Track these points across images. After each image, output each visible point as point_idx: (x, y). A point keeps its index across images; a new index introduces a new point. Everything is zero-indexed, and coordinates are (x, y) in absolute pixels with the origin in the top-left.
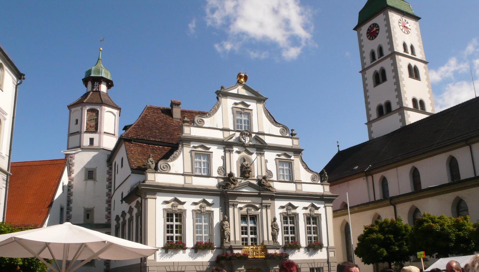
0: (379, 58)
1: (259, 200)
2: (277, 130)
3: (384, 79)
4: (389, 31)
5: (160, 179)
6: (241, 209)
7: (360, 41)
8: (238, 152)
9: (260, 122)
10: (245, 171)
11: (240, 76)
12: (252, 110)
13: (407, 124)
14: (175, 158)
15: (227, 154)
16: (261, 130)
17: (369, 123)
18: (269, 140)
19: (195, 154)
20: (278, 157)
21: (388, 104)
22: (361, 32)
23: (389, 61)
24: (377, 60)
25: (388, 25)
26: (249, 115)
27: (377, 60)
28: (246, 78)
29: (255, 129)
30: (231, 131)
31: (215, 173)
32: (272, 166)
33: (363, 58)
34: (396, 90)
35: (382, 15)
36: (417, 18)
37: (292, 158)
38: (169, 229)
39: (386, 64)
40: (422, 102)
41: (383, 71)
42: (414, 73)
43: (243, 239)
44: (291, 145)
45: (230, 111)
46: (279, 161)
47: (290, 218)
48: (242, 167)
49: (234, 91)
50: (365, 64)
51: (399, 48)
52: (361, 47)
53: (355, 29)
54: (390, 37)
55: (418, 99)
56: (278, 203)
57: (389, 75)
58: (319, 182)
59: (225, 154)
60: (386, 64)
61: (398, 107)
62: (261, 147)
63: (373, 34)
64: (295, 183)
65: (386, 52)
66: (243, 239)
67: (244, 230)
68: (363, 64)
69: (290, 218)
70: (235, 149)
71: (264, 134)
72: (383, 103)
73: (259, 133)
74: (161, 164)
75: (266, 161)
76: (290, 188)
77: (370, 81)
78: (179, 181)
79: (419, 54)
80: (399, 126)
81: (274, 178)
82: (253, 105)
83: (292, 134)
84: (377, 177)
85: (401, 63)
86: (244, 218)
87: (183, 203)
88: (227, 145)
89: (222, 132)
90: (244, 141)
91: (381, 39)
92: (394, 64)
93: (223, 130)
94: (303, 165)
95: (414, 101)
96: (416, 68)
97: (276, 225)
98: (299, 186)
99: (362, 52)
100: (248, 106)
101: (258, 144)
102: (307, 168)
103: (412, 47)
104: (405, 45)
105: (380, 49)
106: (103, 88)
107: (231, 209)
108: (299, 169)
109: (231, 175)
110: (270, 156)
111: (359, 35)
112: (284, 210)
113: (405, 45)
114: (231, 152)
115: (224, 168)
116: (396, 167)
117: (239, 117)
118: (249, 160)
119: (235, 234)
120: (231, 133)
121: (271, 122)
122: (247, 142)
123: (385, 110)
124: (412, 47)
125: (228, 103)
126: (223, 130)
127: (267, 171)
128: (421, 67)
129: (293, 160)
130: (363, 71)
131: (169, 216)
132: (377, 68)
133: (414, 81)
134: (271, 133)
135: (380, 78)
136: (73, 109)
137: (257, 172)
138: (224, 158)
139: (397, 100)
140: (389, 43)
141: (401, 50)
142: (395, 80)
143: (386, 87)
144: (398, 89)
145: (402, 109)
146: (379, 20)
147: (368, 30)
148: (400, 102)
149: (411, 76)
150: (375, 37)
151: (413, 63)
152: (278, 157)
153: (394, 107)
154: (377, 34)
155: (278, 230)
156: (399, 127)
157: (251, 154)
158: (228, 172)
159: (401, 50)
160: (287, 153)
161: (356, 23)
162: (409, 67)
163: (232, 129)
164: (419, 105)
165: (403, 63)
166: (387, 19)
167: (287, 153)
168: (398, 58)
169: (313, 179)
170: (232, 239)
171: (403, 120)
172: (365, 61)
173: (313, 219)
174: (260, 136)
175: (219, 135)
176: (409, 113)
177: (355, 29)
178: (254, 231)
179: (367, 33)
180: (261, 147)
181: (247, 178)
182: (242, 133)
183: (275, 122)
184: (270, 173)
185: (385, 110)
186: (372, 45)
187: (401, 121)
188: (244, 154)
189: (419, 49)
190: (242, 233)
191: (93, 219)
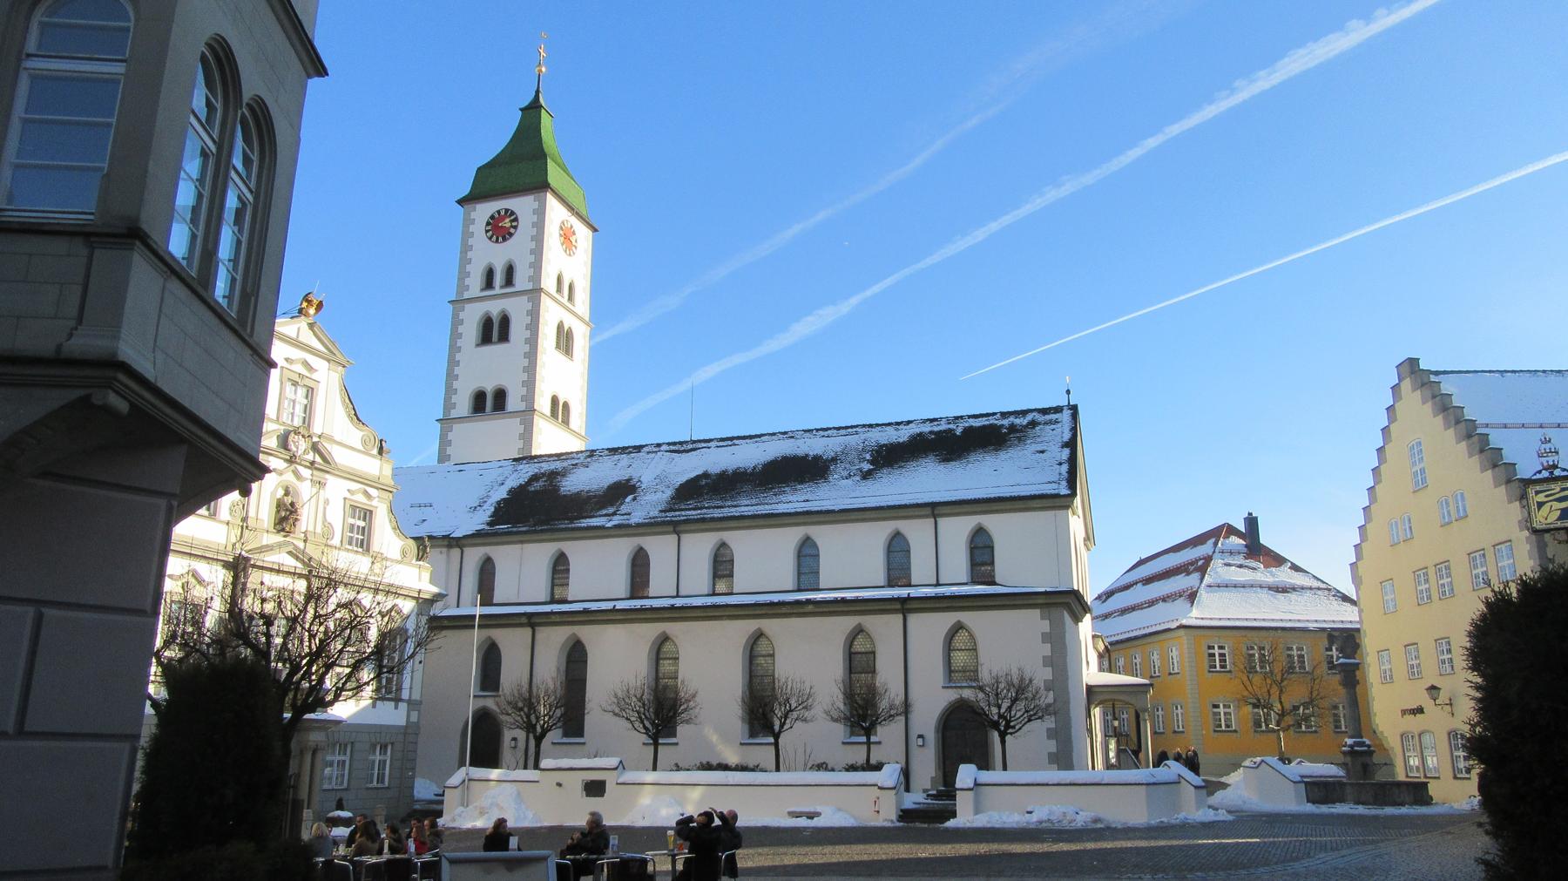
2: (355, 435)
3: (504, 337)
4: (539, 239)
7: (466, 234)
11: (306, 299)
17: (446, 422)
20: (348, 495)
21: (500, 396)
22: (473, 215)
24: (497, 290)
25: (540, 225)
26: (310, 392)
27: (497, 290)
28: (320, 306)
29: (317, 429)
33: (463, 274)
34: (525, 370)
35: (531, 198)
36: (595, 230)
37: (375, 503)
41: (505, 321)
44: (376, 473)
48: (280, 505)
50: (467, 288)
51: (548, 283)
53: (460, 202)
54: (538, 253)
57: (517, 330)
60: (516, 308)
61: (522, 406)
63: (500, 229)
65: (521, 281)
68: (462, 287)
71: (332, 440)
72: (489, 388)
75: (327, 502)
77: (471, 330)
83: (381, 451)
92: (534, 314)
95: (555, 401)
99: (465, 261)
103: (571, 287)
110: (337, 489)
111: (468, 221)
113: (559, 280)
116: (522, 542)
118: (297, 493)
123: (490, 403)
124: (571, 287)
130: (458, 303)
132: (494, 308)
133: (560, 357)
135: (494, 331)
139: (524, 391)
140: (531, 265)
142: (527, 348)
144: (531, 369)
145: (529, 412)
146: (522, 205)
147: (492, 217)
148: (529, 397)
149: (558, 346)
150: (504, 239)
151: (570, 322)
152: (348, 495)
153: (513, 403)
154: (511, 235)
160: (370, 490)
161: (465, 190)
162: (560, 327)
164: (560, 411)
165: (551, 314)
166: (541, 212)
167: (370, 490)
168: (546, 302)
169: (404, 554)
171: (527, 436)
172: (467, 282)
177: (460, 202)
179: (488, 224)
184: (328, 527)
185: (490, 403)
188: (289, 477)
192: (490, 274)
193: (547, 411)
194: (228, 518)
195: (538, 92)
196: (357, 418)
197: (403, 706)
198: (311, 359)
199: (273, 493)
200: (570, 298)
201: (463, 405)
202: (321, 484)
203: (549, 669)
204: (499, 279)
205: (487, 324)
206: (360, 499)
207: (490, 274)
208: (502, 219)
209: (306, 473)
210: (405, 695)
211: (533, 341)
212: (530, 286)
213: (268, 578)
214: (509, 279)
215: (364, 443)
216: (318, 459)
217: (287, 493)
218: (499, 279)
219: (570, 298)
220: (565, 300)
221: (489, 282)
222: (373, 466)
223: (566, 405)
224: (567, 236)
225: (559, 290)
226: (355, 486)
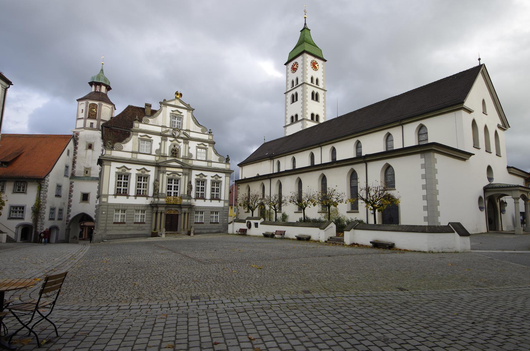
1: (181, 170)
2: (199, 129)
3: (297, 100)
5: (115, 154)
6: (168, 174)
7: (287, 73)
9: (188, 123)
10: (175, 152)
14: (127, 142)
15: (163, 142)
16: (188, 129)
18: (192, 135)
19: (142, 139)
21: (297, 116)
23: (300, 88)
24: (295, 86)
27: (295, 86)
29: (184, 128)
31: (154, 153)
37: (207, 147)
38: (119, 184)
39: (299, 90)
40: (317, 116)
41: (297, 94)
42: (315, 97)
43: (168, 193)
47: (201, 182)
49: (172, 103)
52: (287, 77)
55: (315, 114)
56: (195, 173)
63: (294, 69)
65: (300, 82)
66: (168, 193)
67: (169, 188)
68: (287, 88)
69: (201, 182)
70: (169, 139)
71: (189, 131)
73: (187, 130)
74: (117, 145)
75: (189, 148)
76: (204, 164)
77: (289, 100)
78: (128, 156)
79: (321, 85)
81: (194, 157)
82: (184, 112)
84: (276, 161)
86: (170, 180)
87: (130, 169)
88: (163, 136)
91: (298, 73)
93: (162, 126)
95: (312, 115)
96: (317, 95)
97: (191, 186)
98: (210, 164)
101: (185, 137)
102: (216, 153)
103: (317, 80)
104: (312, 78)
105: (297, 79)
106: (103, 89)
107: (161, 175)
110: (193, 145)
111: (287, 69)
112: (199, 177)
113: (312, 78)
114: (166, 140)
115: (160, 150)
116: (285, 156)
118: (178, 145)
119: (163, 189)
120: (167, 129)
124: (317, 80)
125: (169, 110)
126: (162, 126)
127: (189, 153)
128: (321, 93)
131: (119, 176)
132: (294, 92)
133: (314, 102)
136: (80, 103)
137: (182, 154)
138: (160, 144)
141: (309, 82)
143: (298, 104)
149: (313, 98)
151: (316, 90)
153: (300, 118)
155: (191, 188)
162: (313, 93)
170: (160, 192)
173: (216, 183)
174: (187, 133)
175: (159, 130)
176: (307, 122)
177: (285, 64)
178: (176, 188)
180: (187, 139)
181: (176, 157)
182: (174, 129)
184: (190, 155)
186: (293, 76)
190: (168, 189)
191: (90, 174)
192: (293, 82)
193: (310, 118)
194: (155, 154)
195: (305, 24)
197: (222, 202)
199: (170, 147)
200: (317, 83)
201: (289, 121)
202: (188, 143)
203: (275, 191)
205: (293, 96)
207: (293, 82)
208: (294, 65)
209: (181, 140)
210: (222, 198)
212: (302, 83)
213: (167, 169)
214: (297, 83)
215: (202, 130)
216: (185, 137)
217: (174, 146)
219: (317, 83)
220: (315, 85)
224: (314, 65)
225: (312, 81)
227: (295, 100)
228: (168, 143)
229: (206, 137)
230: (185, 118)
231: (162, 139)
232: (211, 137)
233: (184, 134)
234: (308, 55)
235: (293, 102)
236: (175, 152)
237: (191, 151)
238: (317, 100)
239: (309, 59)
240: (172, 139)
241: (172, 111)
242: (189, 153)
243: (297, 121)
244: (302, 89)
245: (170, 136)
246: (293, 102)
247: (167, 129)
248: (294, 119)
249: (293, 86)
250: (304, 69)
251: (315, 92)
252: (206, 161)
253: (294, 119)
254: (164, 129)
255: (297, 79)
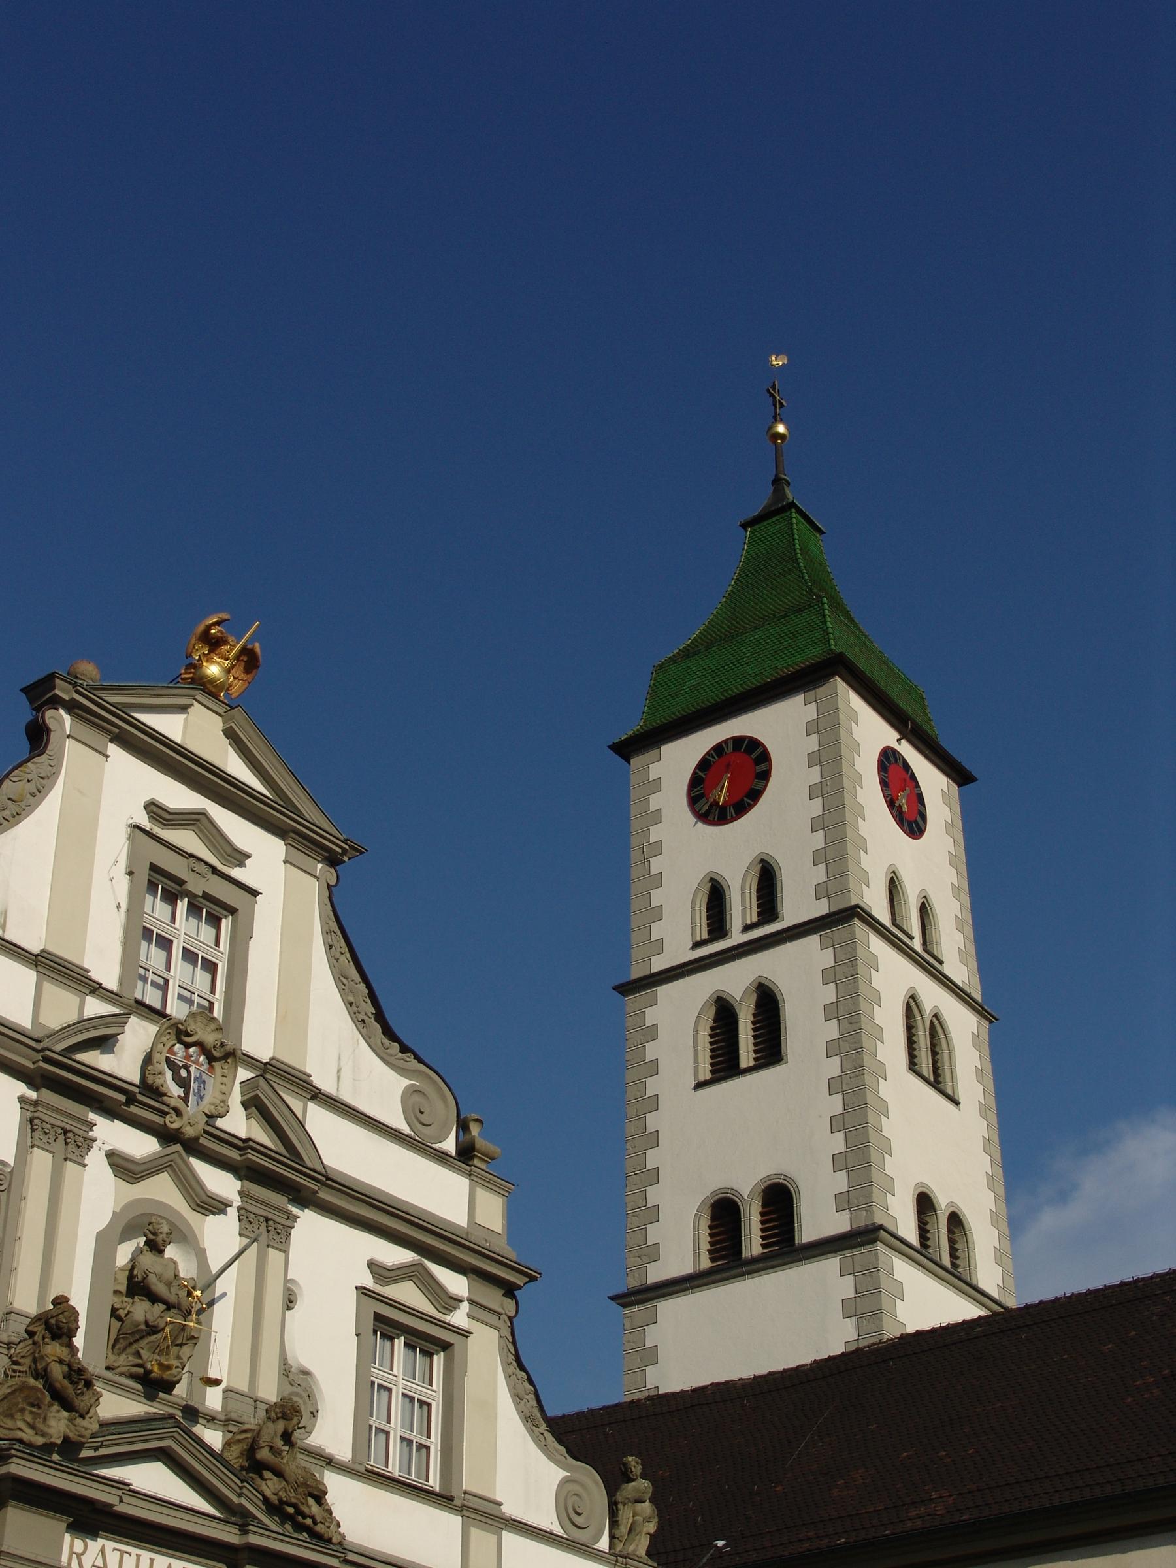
0: (747, 928)
2: (381, 1087)
3: (771, 1050)
8: (122, 1166)
12: (254, 893)
13: (891, 1332)
15: (41, 1161)
16: (289, 1058)
18: (338, 1146)
21: (779, 1200)
23: (811, 953)
25: (830, 756)
30: (96, 989)
32: (325, 1340)
37: (460, 1317)
41: (768, 1003)
45: (111, 853)
46: (384, 1324)
55: (943, 1201)
57: (806, 1026)
58: (604, 1544)
59: (24, 1149)
60: (798, 970)
62: (285, 1181)
64: (461, 1510)
65: (797, 905)
70: (112, 1134)
72: (746, 1184)
73: (269, 1070)
80: (836, 1337)
81: (333, 1431)
82: (265, 859)
83: (466, 1154)
85: (878, 980)
89: (29, 976)
90: (175, 1090)
92: (847, 977)
94: (517, 1397)
100: (240, 858)
104: (894, 887)
105: (767, 880)
108: (491, 1417)
109: (56, 1323)
110: (330, 1259)
113: (894, 887)
114: (76, 1144)
117: (157, 910)
120: (95, 1007)
121: (361, 1023)
122: (191, 1109)
124: (924, 910)
126: (52, 967)
127: (286, 1369)
129: (465, 1334)
132: (734, 981)
134: (347, 1097)
137: (224, 1362)
151: (933, 997)
153: (817, 1219)
156: (838, 1350)
157: (212, 1206)
158: (27, 1300)
159: (883, 914)
162: (912, 1007)
163: (111, 983)
164: (940, 1239)
165: (891, 977)
171: (867, 1301)
180: (285, 1181)
183: (384, 1025)
187: (850, 1309)
189: (959, 937)
192: (716, 896)
193: (909, 1230)
196: (385, 1024)
198: (238, 830)
199: (105, 1243)
201: (679, 1245)
204: (741, 907)
205: (724, 1014)
206: (408, 1293)
207: (716, 896)
209: (220, 1183)
211: (851, 1045)
214: (768, 905)
216: (261, 1135)
218: (741, 907)
221: (717, 925)
222: (442, 1194)
223: (955, 1220)
226: (396, 1255)
227: (746, 1057)
228: (97, 1195)
229: (442, 1194)
230: (268, 917)
231: (34, 1126)
232: (492, 1213)
233: (253, 1104)
234: (856, 702)
235: (725, 1065)
236: (156, 1313)
237: (302, 1354)
238: (936, 1082)
239: (870, 732)
240: (140, 1145)
241: (154, 809)
242: (286, 1369)
243: (785, 1246)
244: (827, 958)
245: (120, 1101)
246: (725, 1065)
247: (95, 1007)
248: (754, 1232)
249: (717, 925)
250: (832, 791)
251: (928, 1008)
252: (443, 1499)
253: (754, 1232)
254: (63, 1009)
255: (767, 880)
